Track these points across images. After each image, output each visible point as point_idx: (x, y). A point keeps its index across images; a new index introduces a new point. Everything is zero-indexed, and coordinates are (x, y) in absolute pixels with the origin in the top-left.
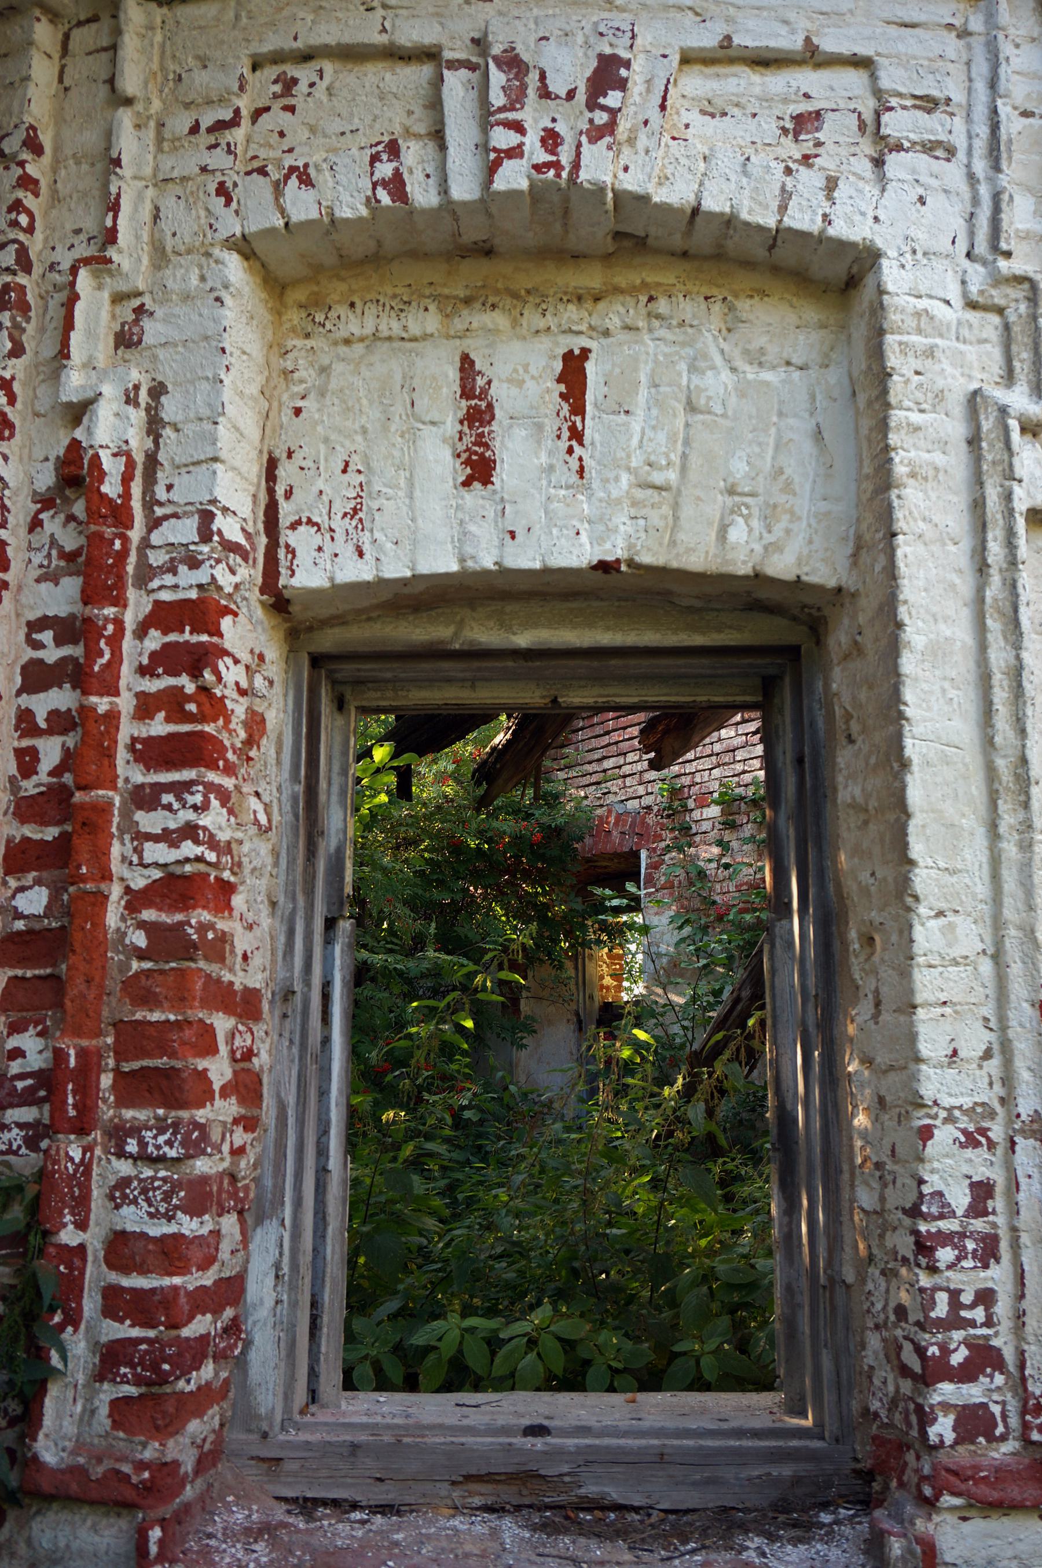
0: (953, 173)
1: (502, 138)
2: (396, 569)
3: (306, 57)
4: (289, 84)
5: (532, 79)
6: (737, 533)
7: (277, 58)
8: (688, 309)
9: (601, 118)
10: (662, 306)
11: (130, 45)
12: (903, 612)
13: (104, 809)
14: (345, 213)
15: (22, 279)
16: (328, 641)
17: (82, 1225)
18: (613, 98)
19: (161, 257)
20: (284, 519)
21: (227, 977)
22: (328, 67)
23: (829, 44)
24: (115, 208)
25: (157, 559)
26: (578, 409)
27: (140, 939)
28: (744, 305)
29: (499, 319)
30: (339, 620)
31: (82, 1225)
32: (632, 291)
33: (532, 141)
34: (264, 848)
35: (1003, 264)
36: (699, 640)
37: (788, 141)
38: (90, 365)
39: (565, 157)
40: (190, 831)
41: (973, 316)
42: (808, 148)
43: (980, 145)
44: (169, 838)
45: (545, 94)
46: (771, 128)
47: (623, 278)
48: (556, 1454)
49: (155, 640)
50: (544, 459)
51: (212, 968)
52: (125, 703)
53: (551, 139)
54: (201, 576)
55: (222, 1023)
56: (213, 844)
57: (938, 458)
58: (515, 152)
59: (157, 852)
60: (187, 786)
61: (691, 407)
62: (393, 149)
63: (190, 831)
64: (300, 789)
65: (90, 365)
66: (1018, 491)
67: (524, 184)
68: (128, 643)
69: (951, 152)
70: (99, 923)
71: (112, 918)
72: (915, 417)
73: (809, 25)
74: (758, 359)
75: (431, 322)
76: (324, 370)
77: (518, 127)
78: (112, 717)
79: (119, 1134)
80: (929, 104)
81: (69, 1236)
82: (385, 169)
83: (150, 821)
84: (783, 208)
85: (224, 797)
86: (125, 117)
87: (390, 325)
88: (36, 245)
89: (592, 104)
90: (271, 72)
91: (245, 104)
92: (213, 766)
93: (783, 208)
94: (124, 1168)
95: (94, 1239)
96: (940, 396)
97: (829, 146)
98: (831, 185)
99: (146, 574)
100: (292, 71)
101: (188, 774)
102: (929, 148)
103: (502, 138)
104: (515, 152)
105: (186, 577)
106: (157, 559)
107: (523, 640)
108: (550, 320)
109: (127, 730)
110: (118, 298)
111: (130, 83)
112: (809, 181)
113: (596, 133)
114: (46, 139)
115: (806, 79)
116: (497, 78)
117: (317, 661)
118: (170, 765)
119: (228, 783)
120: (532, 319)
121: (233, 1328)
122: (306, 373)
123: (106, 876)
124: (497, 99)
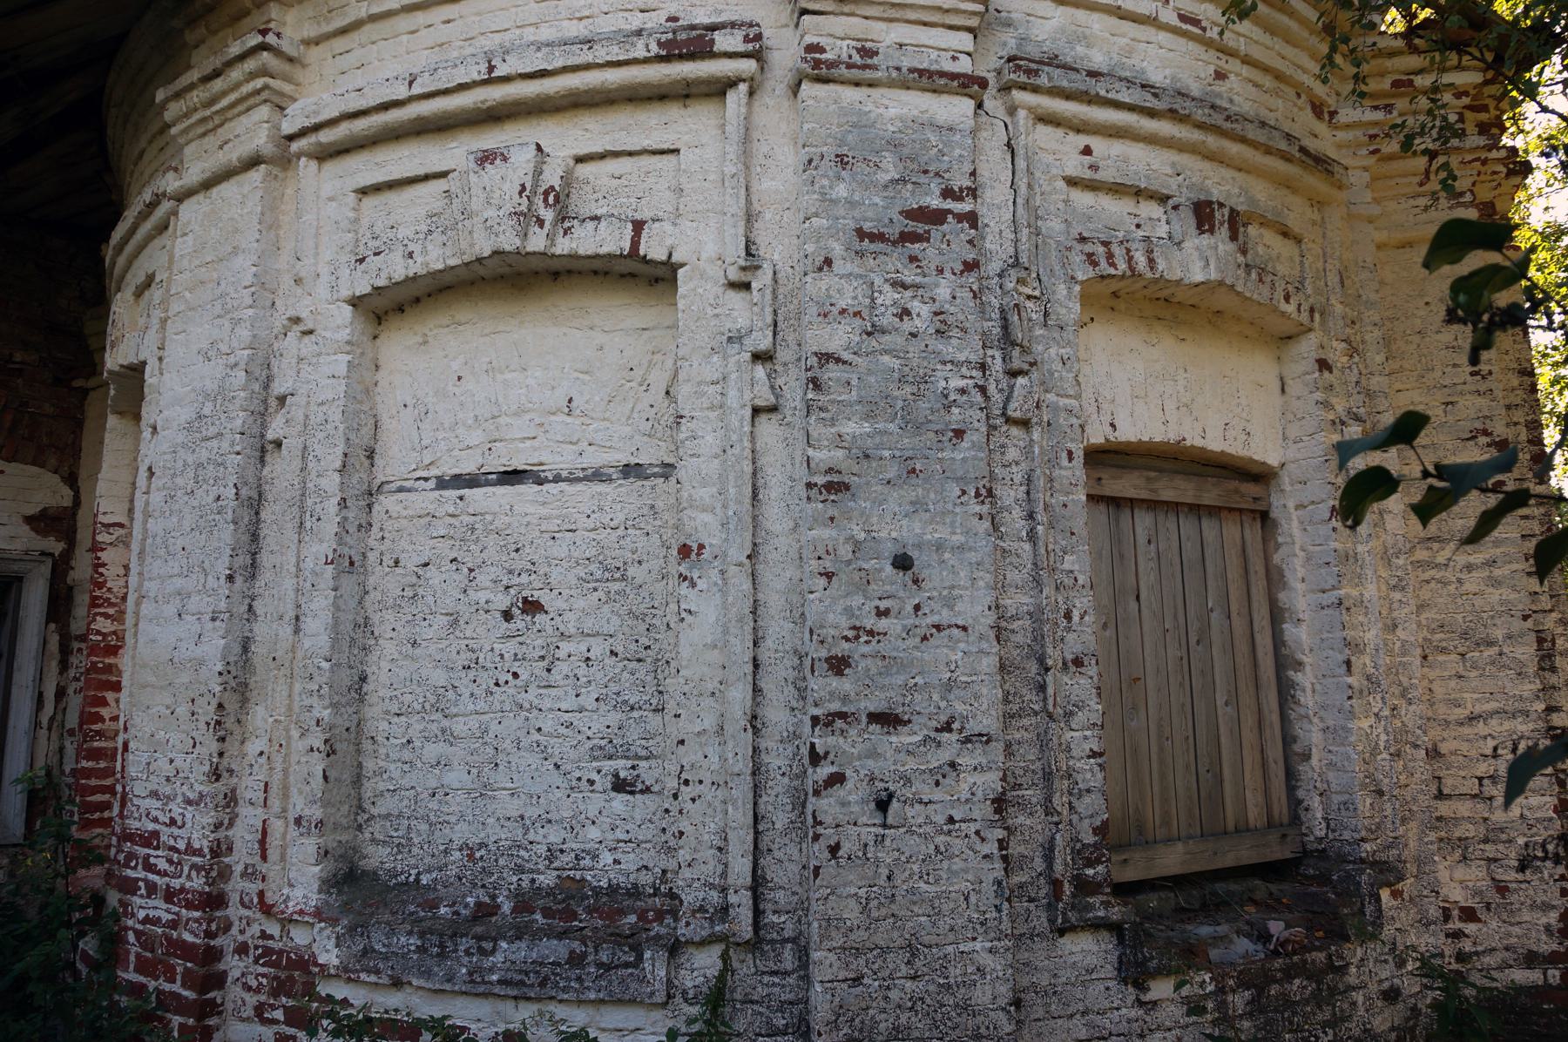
85: (107, 616)
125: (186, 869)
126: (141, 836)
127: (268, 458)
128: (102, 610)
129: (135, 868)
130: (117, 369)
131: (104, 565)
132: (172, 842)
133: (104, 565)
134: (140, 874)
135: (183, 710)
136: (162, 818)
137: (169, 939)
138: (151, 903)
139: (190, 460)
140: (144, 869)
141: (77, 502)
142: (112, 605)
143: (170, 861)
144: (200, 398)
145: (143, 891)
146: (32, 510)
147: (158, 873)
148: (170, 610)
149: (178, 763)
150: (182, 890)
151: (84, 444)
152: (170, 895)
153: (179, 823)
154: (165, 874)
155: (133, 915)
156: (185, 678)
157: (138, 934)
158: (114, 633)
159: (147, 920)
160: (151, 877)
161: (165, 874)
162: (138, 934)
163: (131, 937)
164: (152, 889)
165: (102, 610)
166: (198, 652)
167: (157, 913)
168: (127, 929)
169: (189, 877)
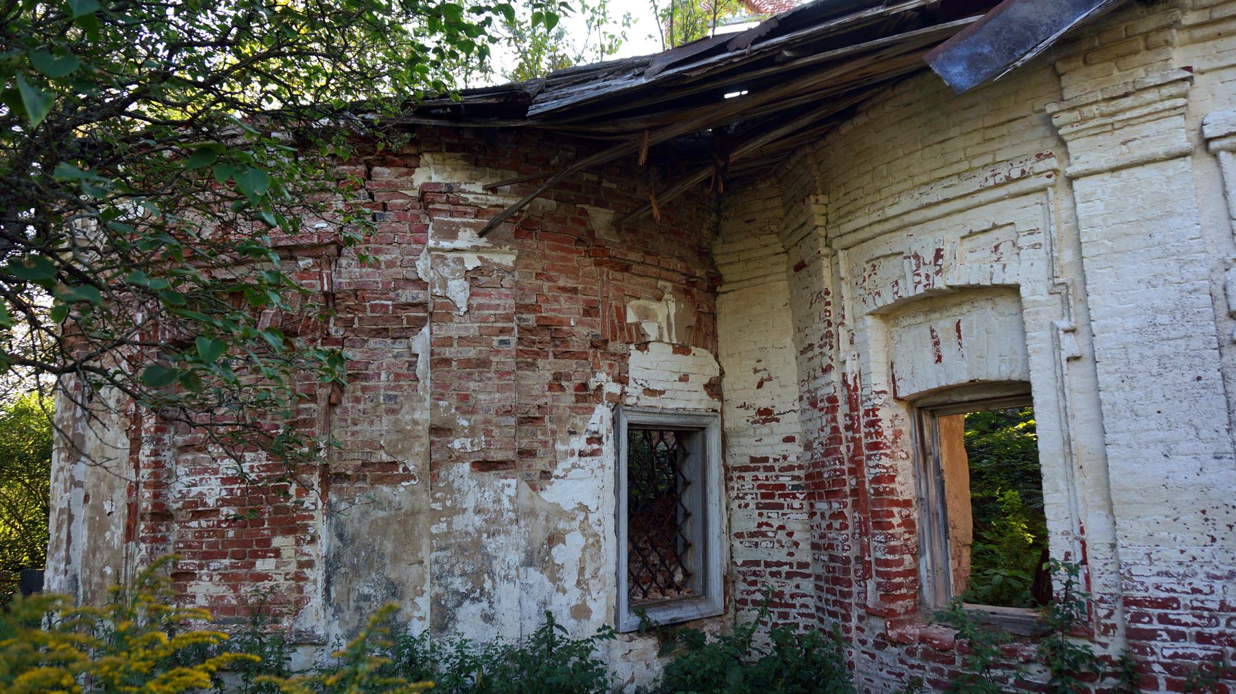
0: (1042, 252)
1: (917, 279)
2: (923, 389)
3: (878, 258)
4: (874, 266)
5: (921, 260)
6: (1003, 368)
7: (872, 260)
8: (982, 303)
9: (938, 268)
10: (976, 305)
11: (841, 262)
12: (1033, 394)
13: (861, 461)
14: (889, 303)
15: (830, 329)
16: (920, 404)
17: (870, 556)
18: (940, 262)
19: (855, 321)
20: (896, 379)
21: (895, 498)
22: (882, 260)
23: (999, 223)
24: (843, 309)
25: (864, 399)
26: (960, 337)
27: (872, 491)
28: (998, 300)
29: (937, 315)
30: (919, 398)
31: (870, 556)
32: (968, 301)
33: (923, 278)
34: (908, 463)
35: (1056, 281)
36: (1011, 393)
37: (993, 255)
38: (844, 351)
39: (931, 282)
40: (877, 466)
41: (1051, 297)
42: (999, 256)
43: (1048, 243)
44: (874, 467)
45: (924, 264)
46: (988, 252)
47: (964, 299)
48: (996, 619)
49: (866, 419)
50: (953, 353)
51: (890, 497)
52: (862, 435)
53: (927, 276)
54: (871, 403)
55: (895, 510)
56: (884, 467)
57: (1043, 345)
58: (919, 283)
59: (873, 471)
60: (875, 455)
61: (988, 333)
62: (897, 283)
63: (877, 466)
64: (919, 445)
65: (844, 351)
66: (1063, 353)
67: (923, 291)
68: (861, 420)
69: (1040, 245)
70: (864, 488)
71: (867, 486)
72: (1034, 334)
73: (993, 218)
74: (1002, 314)
75: (921, 319)
76: (900, 336)
77: (919, 275)
78: (860, 439)
79: (874, 535)
80: (1031, 232)
81: (867, 558)
82: (895, 289)
83: (871, 463)
84: (991, 279)
86: (843, 284)
87: (912, 321)
88: (832, 318)
89: (935, 265)
90: (870, 264)
91: (866, 275)
92: (882, 448)
93: (991, 279)
94: (876, 543)
95: (872, 559)
96: (1041, 326)
97: (1005, 253)
98: (1004, 266)
99: (862, 402)
100: (874, 262)
101: (875, 452)
102: (1034, 246)
103: (917, 279)
104: (919, 283)
105: (869, 403)
106: (864, 399)
107: (966, 398)
108: (950, 313)
109: (864, 441)
110: (849, 331)
111: (843, 274)
112: (997, 267)
113: (937, 273)
114: (830, 290)
115: (996, 233)
116: (913, 261)
117: (920, 409)
118: (872, 450)
119: (888, 451)
120: (945, 314)
121: (915, 581)
122: (897, 338)
123: (864, 477)
124: (914, 268)
125: (1223, 622)
126: (1151, 602)
127: (1224, 351)
128: (883, 451)
129: (1150, 622)
130: (944, 287)
131: (880, 420)
132: (1196, 604)
133: (880, 420)
134: (1156, 625)
135: (1192, 518)
136: (1179, 588)
137: (1216, 668)
138: (1177, 645)
139: (1149, 353)
140: (1160, 622)
141: (722, 373)
142: (888, 447)
143: (1201, 617)
144: (1150, 312)
145: (1165, 636)
146: (706, 381)
147: (1186, 625)
148: (1155, 451)
149: (1194, 551)
150: (1221, 634)
151: (720, 332)
152: (1201, 638)
153: (1207, 590)
154: (1195, 625)
155: (1153, 653)
156: (1189, 496)
157: (1166, 667)
158: (891, 466)
159: (1175, 655)
160: (1171, 627)
161: (1195, 625)
162: (1162, 664)
163: (1157, 668)
164: (1176, 637)
165: (883, 451)
166: (1203, 479)
167: (1188, 651)
168: (1149, 663)
169: (1228, 625)
